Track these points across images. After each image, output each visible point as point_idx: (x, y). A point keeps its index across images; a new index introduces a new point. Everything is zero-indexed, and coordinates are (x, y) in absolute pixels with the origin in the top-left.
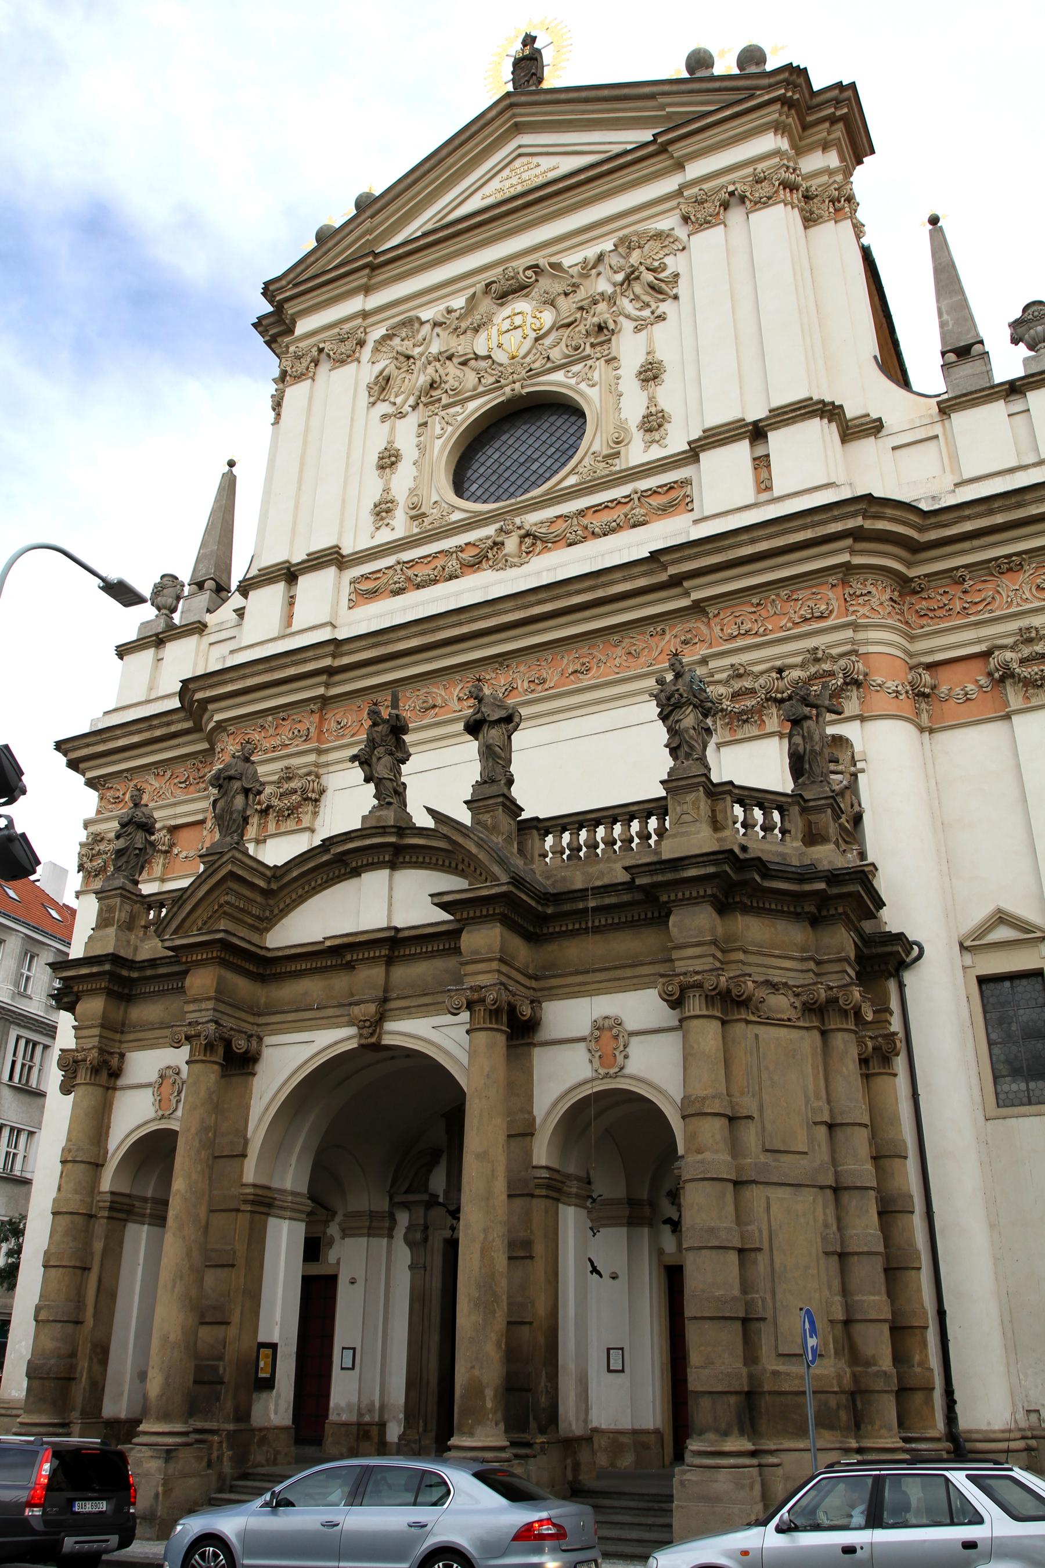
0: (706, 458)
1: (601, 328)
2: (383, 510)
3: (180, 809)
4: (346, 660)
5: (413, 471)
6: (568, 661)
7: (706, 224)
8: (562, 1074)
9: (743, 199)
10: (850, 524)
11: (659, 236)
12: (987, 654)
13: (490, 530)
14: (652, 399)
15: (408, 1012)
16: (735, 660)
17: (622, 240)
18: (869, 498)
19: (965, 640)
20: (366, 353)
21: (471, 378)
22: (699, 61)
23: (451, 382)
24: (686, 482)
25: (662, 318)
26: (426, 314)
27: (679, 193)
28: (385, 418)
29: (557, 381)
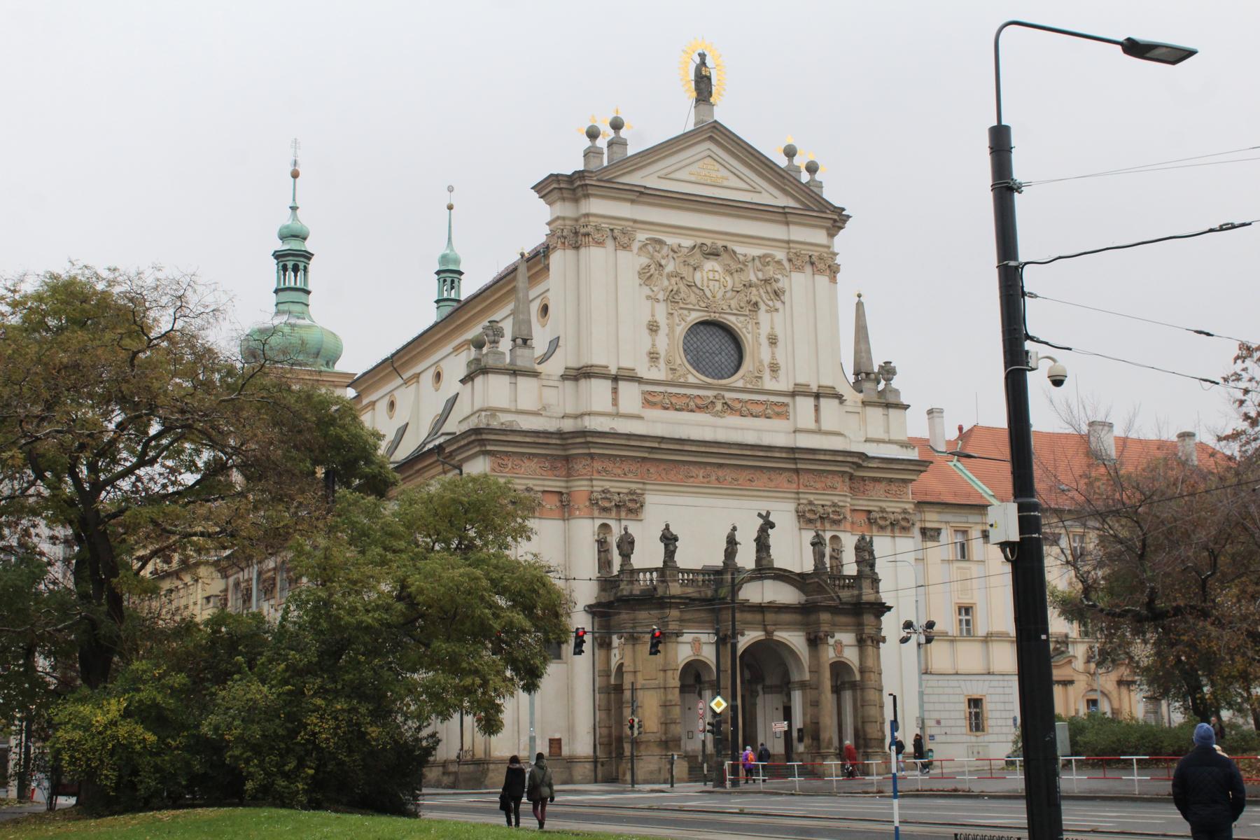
0: (798, 399)
1: (756, 304)
2: (653, 357)
3: (547, 483)
4: (663, 446)
5: (666, 340)
6: (745, 475)
7: (800, 269)
8: (829, 654)
9: (812, 264)
10: (855, 460)
11: (779, 262)
12: (869, 512)
13: (710, 393)
14: (773, 353)
15: (781, 630)
16: (812, 497)
17: (765, 256)
18: (863, 454)
19: (863, 504)
20: (636, 246)
21: (693, 299)
22: (790, 152)
23: (682, 295)
24: (786, 405)
25: (777, 310)
26: (671, 240)
27: (788, 242)
28: (648, 297)
29: (732, 320)
